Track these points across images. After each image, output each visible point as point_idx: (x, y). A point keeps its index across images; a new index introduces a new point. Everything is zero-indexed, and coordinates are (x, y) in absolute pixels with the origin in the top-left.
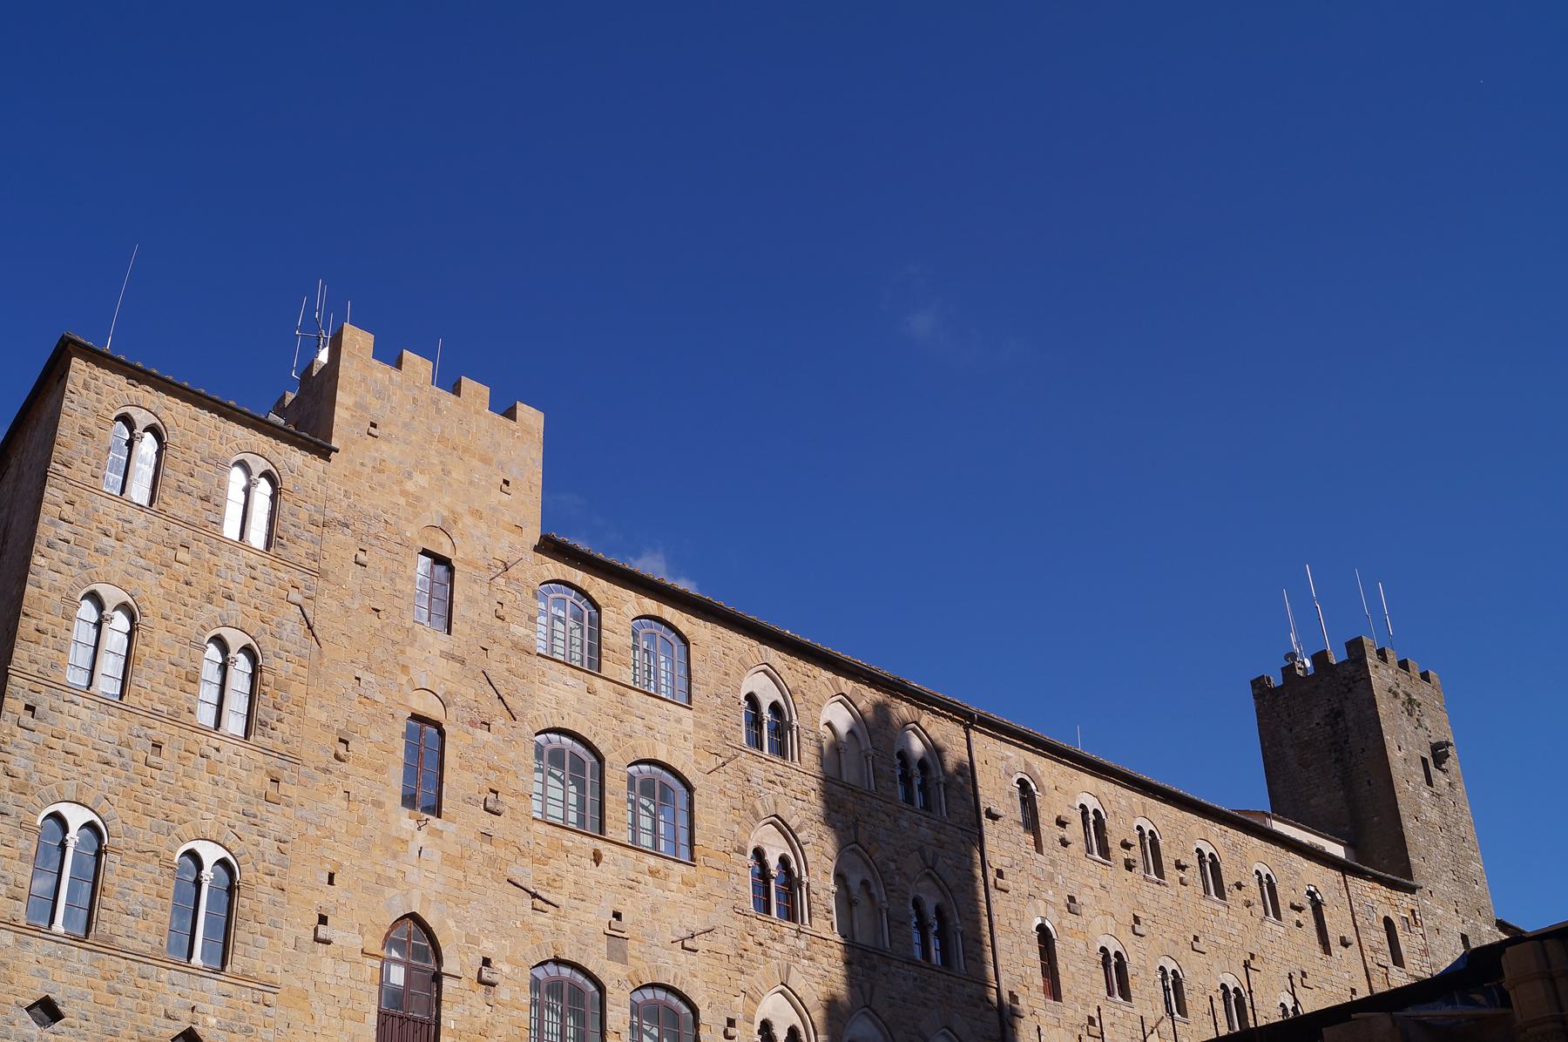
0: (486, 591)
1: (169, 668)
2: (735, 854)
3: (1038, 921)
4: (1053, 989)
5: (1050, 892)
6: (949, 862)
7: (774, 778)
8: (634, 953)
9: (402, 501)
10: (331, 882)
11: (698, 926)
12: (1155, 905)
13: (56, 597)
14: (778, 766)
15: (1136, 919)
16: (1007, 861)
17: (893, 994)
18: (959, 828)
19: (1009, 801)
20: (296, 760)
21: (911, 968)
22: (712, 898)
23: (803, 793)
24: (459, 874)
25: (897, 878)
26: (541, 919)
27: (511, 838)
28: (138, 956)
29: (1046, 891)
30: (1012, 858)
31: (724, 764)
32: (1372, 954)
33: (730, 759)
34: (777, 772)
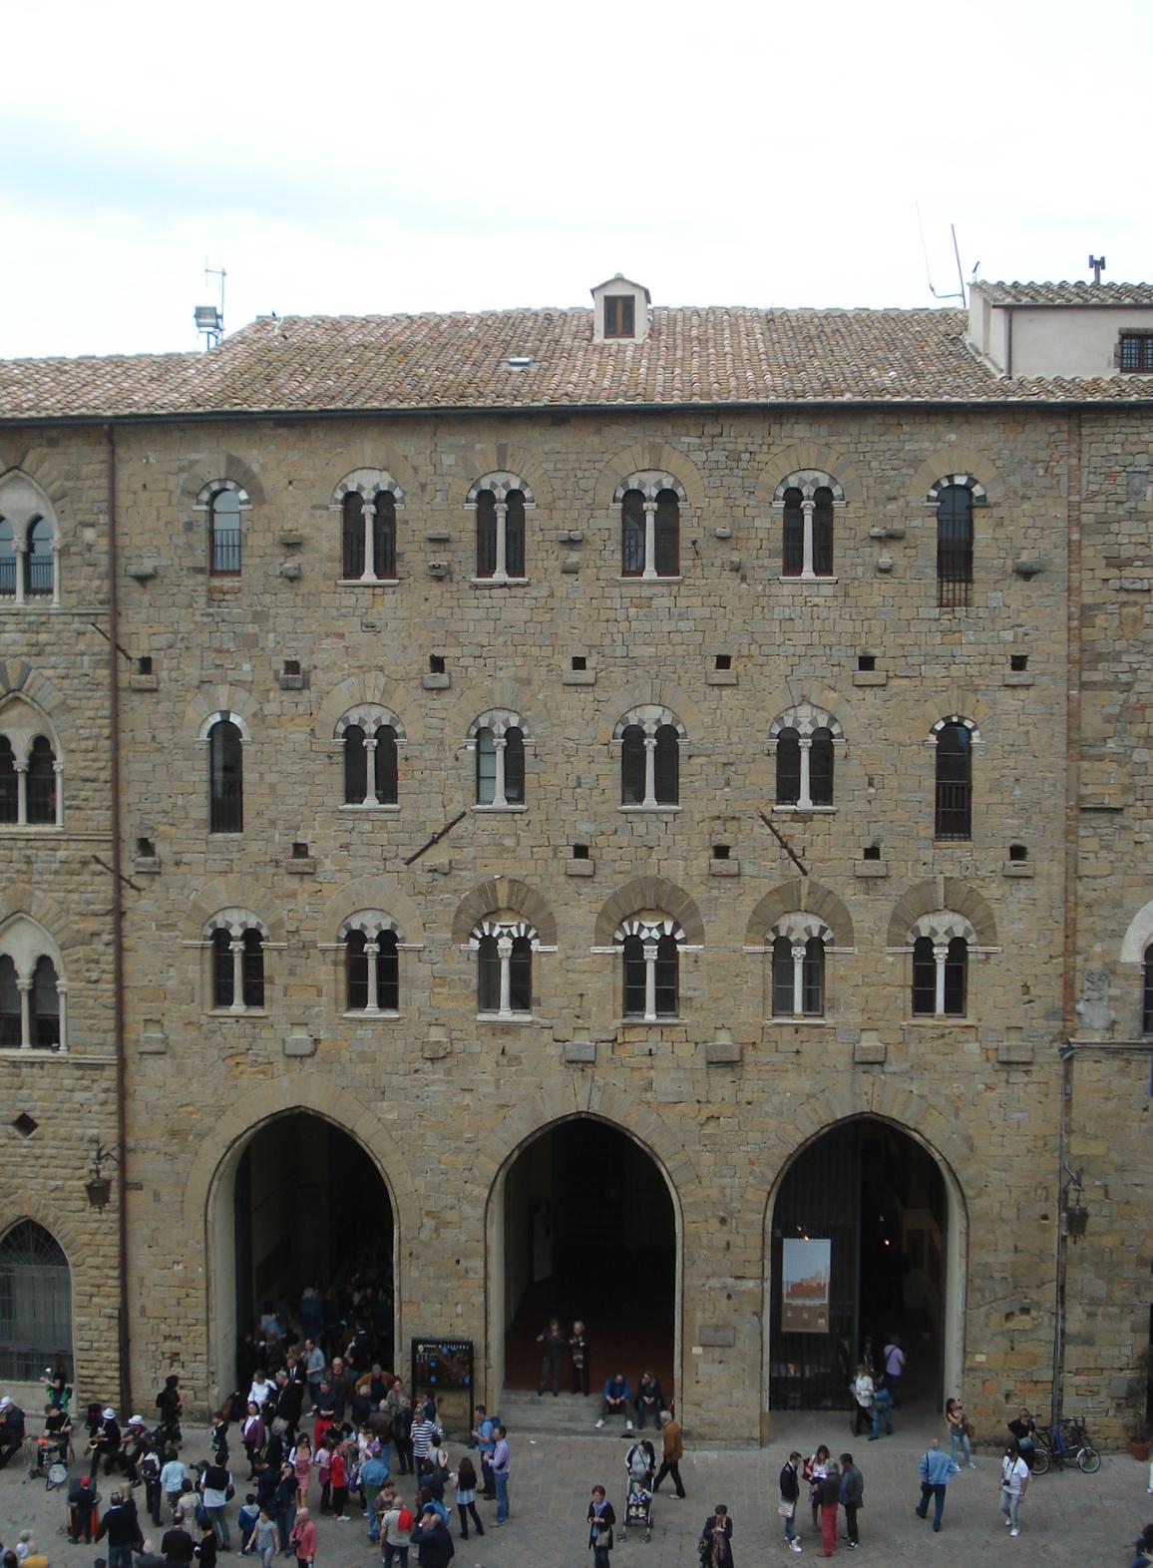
3: (217, 718)
4: (226, 812)
5: (247, 667)
6: (49, 673)
12: (490, 626)
15: (437, 664)
16: (160, 641)
18: (73, 615)
19: (181, 540)
29: (237, 667)
30: (176, 632)
32: (1114, 572)
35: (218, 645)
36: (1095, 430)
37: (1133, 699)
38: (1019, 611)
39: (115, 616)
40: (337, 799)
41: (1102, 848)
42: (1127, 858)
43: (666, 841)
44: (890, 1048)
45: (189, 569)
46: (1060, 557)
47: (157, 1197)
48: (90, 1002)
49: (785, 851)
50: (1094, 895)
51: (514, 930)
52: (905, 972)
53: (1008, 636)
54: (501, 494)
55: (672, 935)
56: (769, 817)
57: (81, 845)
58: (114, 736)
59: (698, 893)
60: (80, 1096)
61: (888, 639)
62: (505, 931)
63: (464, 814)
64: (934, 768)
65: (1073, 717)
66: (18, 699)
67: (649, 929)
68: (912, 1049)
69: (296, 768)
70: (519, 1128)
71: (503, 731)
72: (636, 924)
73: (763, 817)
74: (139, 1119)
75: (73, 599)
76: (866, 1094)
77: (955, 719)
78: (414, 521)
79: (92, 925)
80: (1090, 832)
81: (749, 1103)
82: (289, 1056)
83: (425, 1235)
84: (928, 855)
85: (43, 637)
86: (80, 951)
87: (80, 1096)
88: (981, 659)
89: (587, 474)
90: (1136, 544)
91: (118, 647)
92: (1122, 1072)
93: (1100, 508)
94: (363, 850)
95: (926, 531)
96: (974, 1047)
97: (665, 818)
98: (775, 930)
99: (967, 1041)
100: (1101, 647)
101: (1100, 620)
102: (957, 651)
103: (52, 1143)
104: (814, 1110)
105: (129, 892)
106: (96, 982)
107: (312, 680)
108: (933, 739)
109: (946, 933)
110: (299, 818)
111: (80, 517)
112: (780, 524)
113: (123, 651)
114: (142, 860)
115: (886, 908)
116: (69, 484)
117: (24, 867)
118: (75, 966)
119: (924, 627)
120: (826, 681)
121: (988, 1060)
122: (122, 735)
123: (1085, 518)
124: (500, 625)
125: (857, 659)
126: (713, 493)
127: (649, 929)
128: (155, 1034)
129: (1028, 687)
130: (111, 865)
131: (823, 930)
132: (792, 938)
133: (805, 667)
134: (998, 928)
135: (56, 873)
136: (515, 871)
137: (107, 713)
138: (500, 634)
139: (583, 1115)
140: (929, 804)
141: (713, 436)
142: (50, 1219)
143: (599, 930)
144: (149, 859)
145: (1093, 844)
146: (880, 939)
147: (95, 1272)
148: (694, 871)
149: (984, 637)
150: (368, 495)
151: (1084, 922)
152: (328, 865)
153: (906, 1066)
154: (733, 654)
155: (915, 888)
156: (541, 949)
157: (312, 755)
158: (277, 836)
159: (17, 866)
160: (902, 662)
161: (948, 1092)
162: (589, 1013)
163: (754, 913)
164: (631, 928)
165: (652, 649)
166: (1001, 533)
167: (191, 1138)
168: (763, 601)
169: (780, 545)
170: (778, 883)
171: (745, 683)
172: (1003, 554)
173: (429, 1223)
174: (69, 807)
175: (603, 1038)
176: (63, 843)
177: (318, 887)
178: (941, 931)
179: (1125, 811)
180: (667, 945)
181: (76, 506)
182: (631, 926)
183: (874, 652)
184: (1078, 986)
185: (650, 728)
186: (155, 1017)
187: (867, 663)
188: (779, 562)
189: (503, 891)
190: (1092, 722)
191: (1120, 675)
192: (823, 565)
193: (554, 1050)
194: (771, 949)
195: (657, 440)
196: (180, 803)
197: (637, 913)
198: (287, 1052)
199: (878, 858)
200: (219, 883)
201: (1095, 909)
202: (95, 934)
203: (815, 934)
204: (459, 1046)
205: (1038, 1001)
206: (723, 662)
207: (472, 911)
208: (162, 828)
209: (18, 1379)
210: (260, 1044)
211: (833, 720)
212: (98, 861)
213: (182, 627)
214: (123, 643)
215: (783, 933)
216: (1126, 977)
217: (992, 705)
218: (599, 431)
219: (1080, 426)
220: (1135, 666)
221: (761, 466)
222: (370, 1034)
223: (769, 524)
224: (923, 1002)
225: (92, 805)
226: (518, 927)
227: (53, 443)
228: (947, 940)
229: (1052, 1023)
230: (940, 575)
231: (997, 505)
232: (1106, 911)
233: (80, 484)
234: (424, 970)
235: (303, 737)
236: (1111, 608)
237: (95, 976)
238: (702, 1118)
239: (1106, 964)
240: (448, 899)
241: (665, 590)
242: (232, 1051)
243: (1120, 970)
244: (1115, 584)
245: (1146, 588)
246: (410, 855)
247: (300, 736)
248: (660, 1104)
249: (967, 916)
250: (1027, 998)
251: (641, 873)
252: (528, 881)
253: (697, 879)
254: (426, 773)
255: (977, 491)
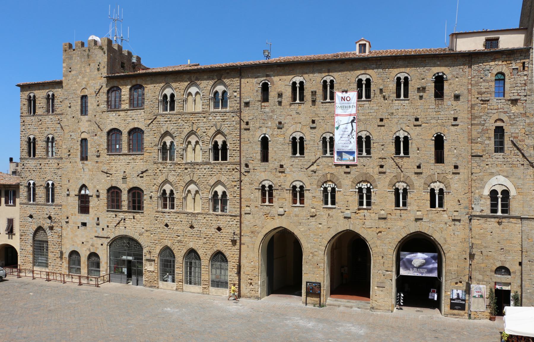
0: (95, 99)
1: (40, 148)
2: (154, 147)
3: (263, 135)
4: (265, 158)
6: (226, 126)
7: (166, 119)
8: (128, 181)
9: (77, 85)
10: (69, 182)
11: (144, 170)
13: (24, 141)
14: (168, 115)
15: (313, 122)
16: (251, 118)
17: (200, 175)
19: (255, 94)
20: (62, 159)
21: (208, 165)
22: (148, 161)
23: (176, 121)
24: (91, 173)
25: (206, 138)
26: (109, 178)
27: (102, 161)
28: (42, 205)
31: (152, 122)
32: (480, 96)
33: (154, 119)
34: (168, 117)
35: (263, 118)
36: (476, 60)
37: (485, 127)
38: (455, 106)
39: (241, 112)
40: (290, 154)
41: (478, 166)
42: (484, 168)
43: (368, 164)
44: (424, 215)
45: (257, 101)
46: (466, 92)
47: (248, 247)
48: (234, 201)
49: (397, 167)
50: (476, 178)
51: (331, 186)
52: (428, 196)
53: (452, 112)
54: (328, 81)
55: (370, 187)
56: (393, 158)
57: (232, 165)
58: (240, 140)
59: (376, 176)
60: (231, 223)
61: (422, 113)
62: (329, 186)
63: (320, 157)
64: (434, 145)
65: (470, 132)
66: (219, 132)
67: (364, 186)
68: (430, 216)
69: (281, 147)
70: (333, 233)
71: (329, 137)
72: (361, 184)
73: (392, 158)
74: (244, 228)
75: (232, 109)
76: (418, 226)
77: (439, 134)
78: (308, 89)
79: (235, 184)
80: (474, 161)
81: (389, 228)
82: (279, 215)
83: (310, 258)
84: (433, 167)
85: (225, 118)
86: (232, 190)
87: (231, 223)
88: (446, 118)
89: (349, 75)
90: (486, 88)
91: (241, 119)
92: (485, 223)
93: (476, 79)
94: (296, 166)
95: (431, 87)
96: (446, 216)
97: (368, 158)
98: (394, 185)
99: (444, 214)
100: (476, 115)
101: (476, 108)
102: (439, 116)
103: (225, 233)
104: (405, 230)
105: (242, 176)
106: (235, 197)
107: (285, 126)
108: (433, 138)
109: (438, 187)
110: (281, 159)
111: (233, 90)
112: (395, 86)
113: (243, 120)
114: (246, 168)
115: (423, 181)
116: (231, 82)
117: (220, 170)
118: (231, 193)
119: (431, 110)
120: (407, 124)
121: (449, 219)
122: (242, 140)
123: (472, 82)
124: (328, 112)
125: (414, 119)
126: (379, 78)
127: (364, 186)
128: (248, 208)
129: (457, 125)
130: (239, 170)
131: (406, 187)
132: (399, 188)
133: (401, 121)
134: (451, 186)
135: (227, 172)
136: (331, 172)
137: (239, 135)
138: (328, 114)
139: (348, 231)
140: (433, 155)
141: (379, 65)
142: (224, 251)
143: (352, 186)
144: (248, 168)
145: (475, 165)
146: (421, 188)
147: (234, 263)
148: (375, 171)
149: (446, 113)
150: (298, 82)
151: (474, 185)
152: (287, 170)
153: (428, 220)
154: (384, 118)
155: (430, 176)
156: (338, 190)
157: (284, 144)
158: (276, 163)
159: (218, 170)
160: (426, 119)
161: (439, 227)
162: (350, 205)
163: (390, 181)
164: (360, 185)
165: (364, 117)
166: (451, 87)
167: (256, 233)
168: (391, 105)
169: (395, 91)
170: (395, 174)
171: (386, 125)
172: (451, 92)
173: (311, 255)
174: (230, 156)
175: (353, 212)
176: (229, 165)
177: (286, 175)
178: (437, 187)
179: (483, 156)
180: (368, 190)
181: (233, 87)
182: (360, 185)
183: (418, 117)
184: (472, 201)
185: (364, 136)
186: (248, 205)
187: (417, 120)
188: (395, 95)
189: (329, 176)
190: (474, 133)
191: (481, 122)
192: (406, 95)
193: (341, 214)
194: (394, 191)
195: (366, 66)
196: (254, 155)
197: (361, 182)
198: (278, 214)
199: (420, 168)
200: (263, 174)
201: (476, 181)
202: (235, 186)
203: (405, 187)
204: (318, 213)
205: (462, 204)
206: (381, 120)
207: (322, 181)
208: (250, 161)
209: (216, 287)
210: (272, 212)
211: (409, 134)
212: (236, 169)
213: (256, 114)
214: (242, 118)
215: (397, 187)
216: (485, 198)
217: (449, 130)
218: (352, 65)
219: (472, 59)
220: (485, 119)
221: (391, 72)
222: (297, 210)
223: (393, 86)
224: (433, 205)
225: (235, 156)
226: (332, 185)
227: (228, 73)
228: (438, 189)
229: (466, 210)
230: (435, 97)
231: (450, 80)
232: (479, 182)
233: (234, 82)
234: (311, 195)
235: (282, 139)
236: (479, 105)
237: (235, 195)
238: (377, 232)
239: (479, 195)
240: (315, 177)
241: (367, 102)
242: (266, 213)
243: (483, 197)
244: (480, 99)
245: (488, 99)
246: (307, 167)
247: (281, 139)
248: (367, 228)
249: (443, 183)
250: (459, 204)
251: (362, 172)
252: (334, 174)
253: (376, 173)
254: (311, 148)
255: (445, 76)
